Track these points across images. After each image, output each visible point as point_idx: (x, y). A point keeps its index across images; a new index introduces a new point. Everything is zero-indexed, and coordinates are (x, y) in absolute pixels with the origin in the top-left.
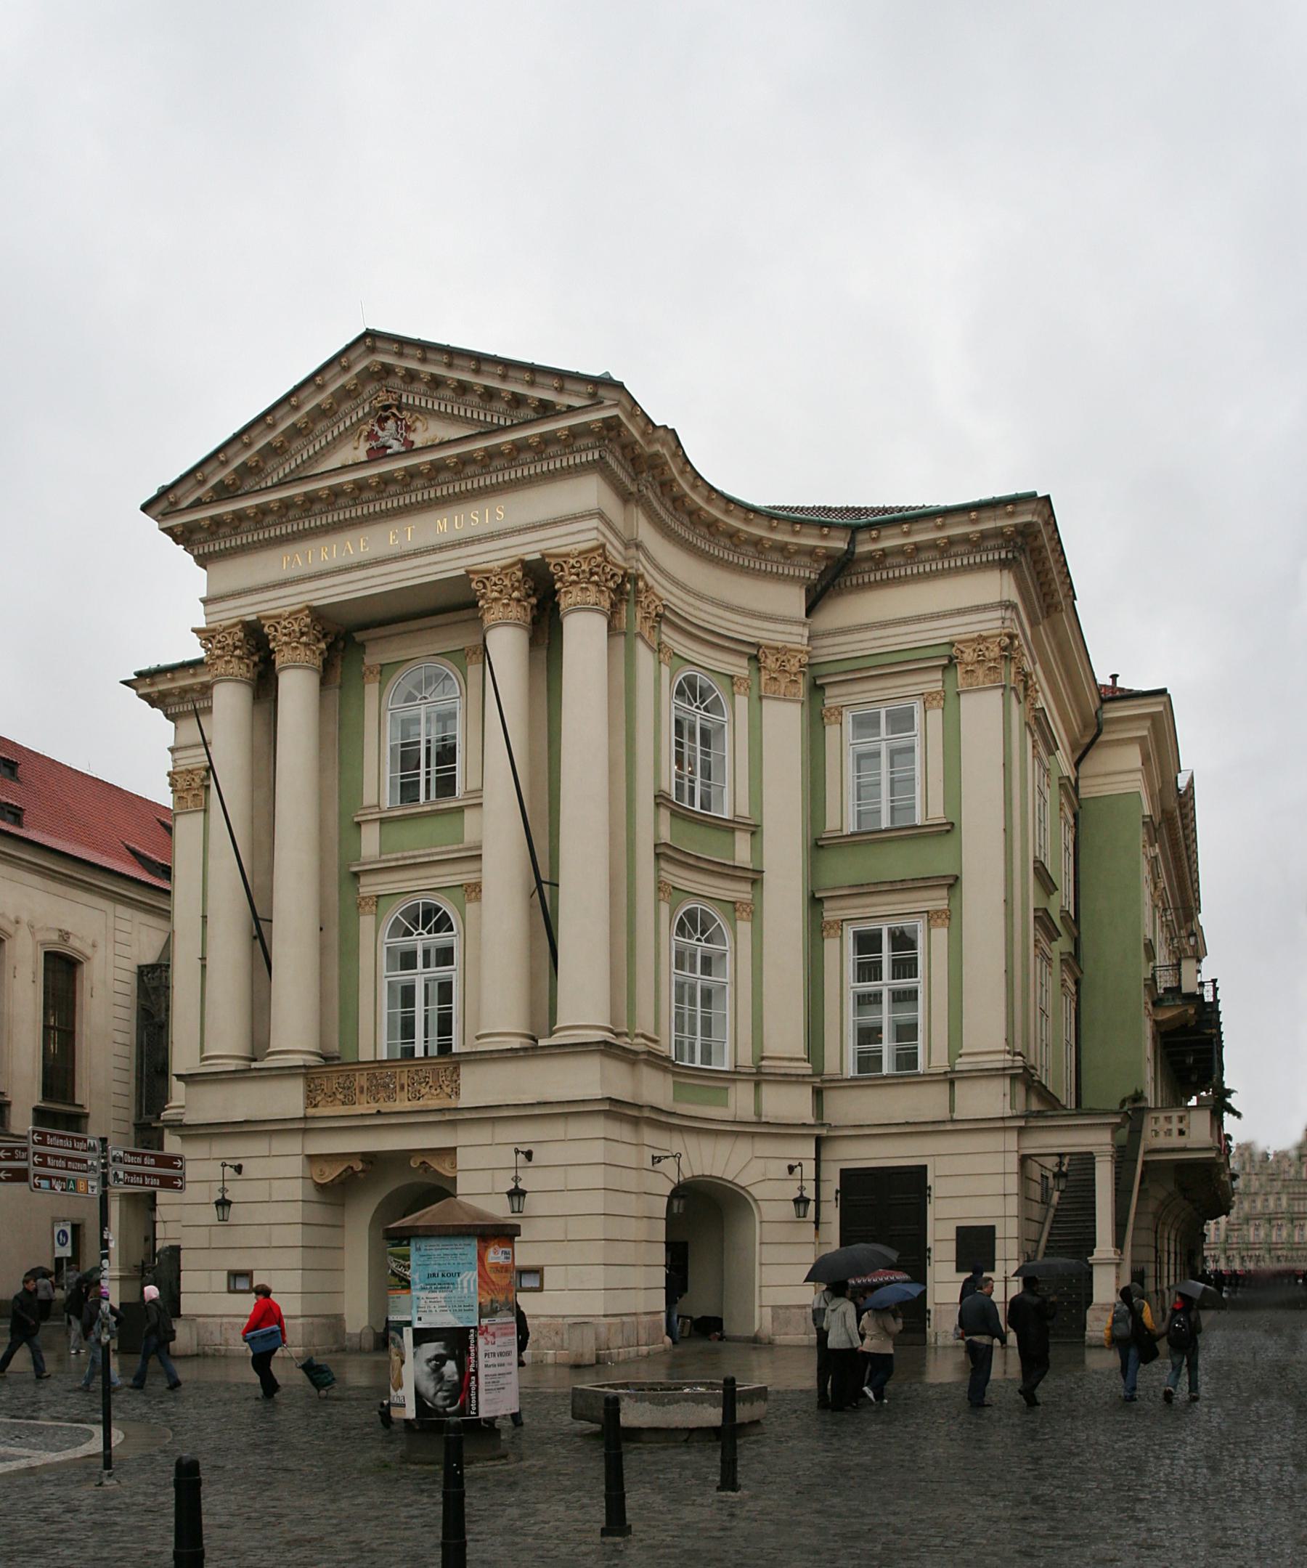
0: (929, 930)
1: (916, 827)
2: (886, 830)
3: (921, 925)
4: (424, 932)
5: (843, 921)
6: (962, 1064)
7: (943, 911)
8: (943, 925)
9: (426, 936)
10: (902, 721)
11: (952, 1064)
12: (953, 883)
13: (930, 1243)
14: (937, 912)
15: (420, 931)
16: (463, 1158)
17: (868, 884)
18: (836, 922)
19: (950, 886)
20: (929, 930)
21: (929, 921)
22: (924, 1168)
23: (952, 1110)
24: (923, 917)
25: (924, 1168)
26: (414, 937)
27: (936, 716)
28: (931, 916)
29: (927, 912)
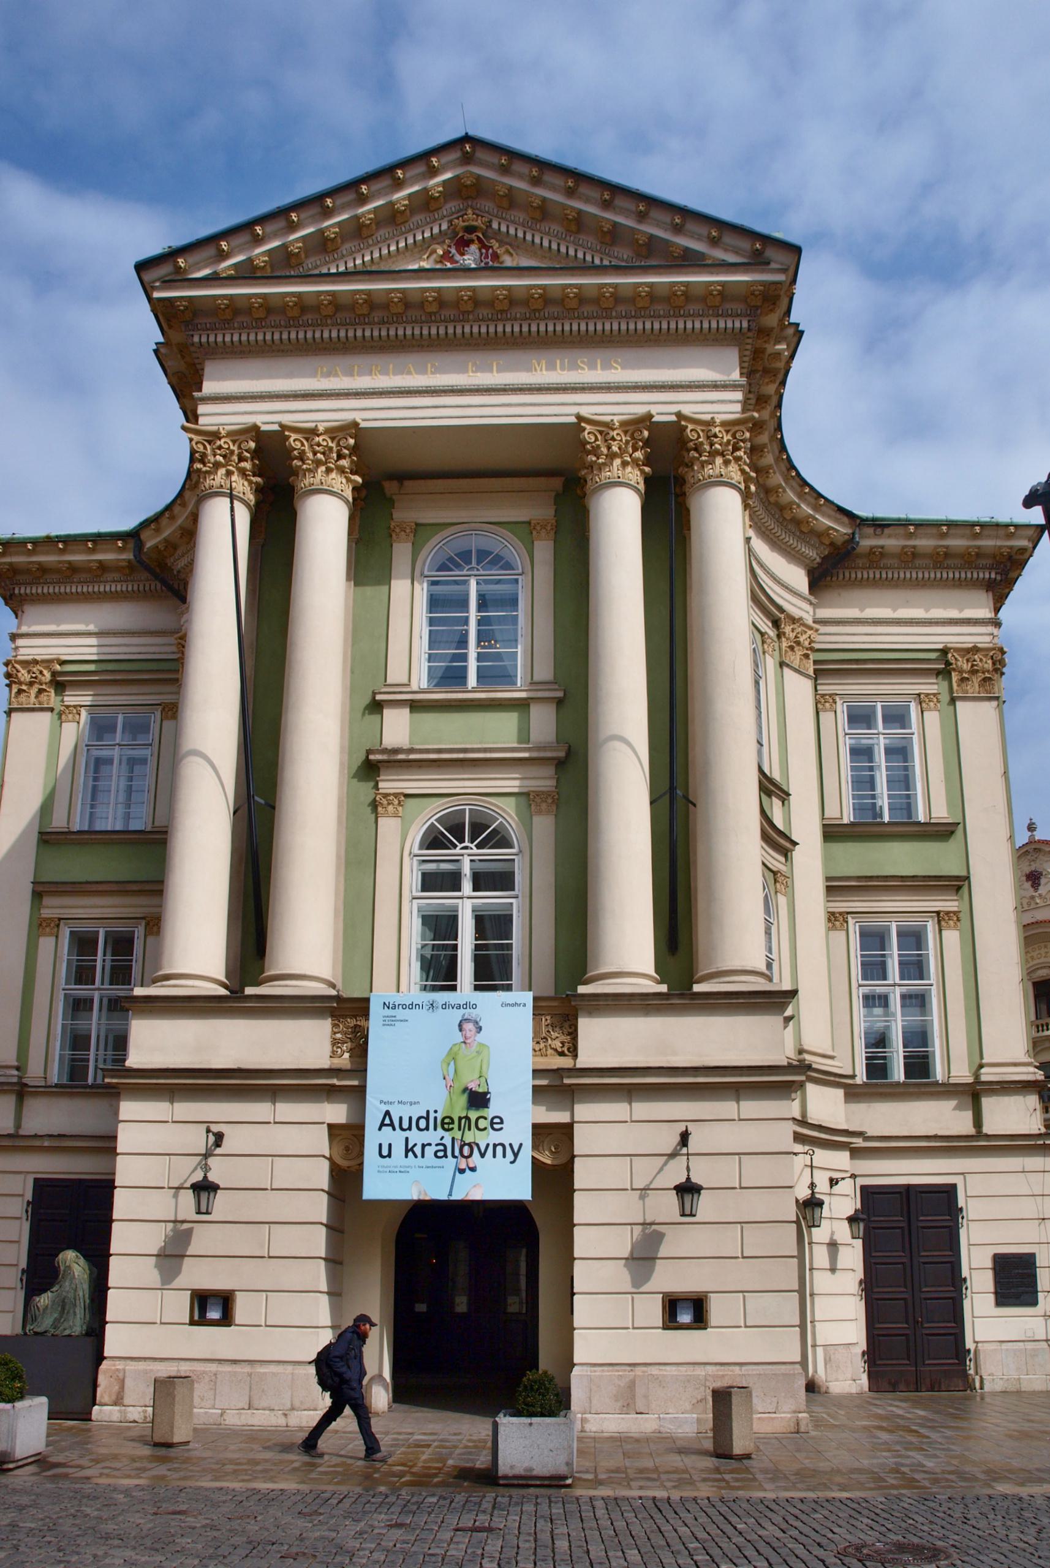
0: (940, 931)
1: (919, 823)
2: (889, 824)
3: (931, 927)
4: (472, 846)
5: (848, 913)
6: (987, 1075)
7: (955, 913)
8: (955, 927)
9: (475, 851)
10: (897, 717)
11: (977, 1075)
12: (958, 884)
13: (965, 1273)
14: (948, 913)
15: (466, 844)
16: (582, 1142)
17: (878, 877)
18: (841, 913)
19: (958, 888)
20: (940, 931)
21: (939, 922)
22: (954, 1187)
23: (978, 1122)
24: (931, 917)
25: (954, 1187)
26: (458, 851)
27: (932, 718)
28: (940, 917)
29: (938, 913)
